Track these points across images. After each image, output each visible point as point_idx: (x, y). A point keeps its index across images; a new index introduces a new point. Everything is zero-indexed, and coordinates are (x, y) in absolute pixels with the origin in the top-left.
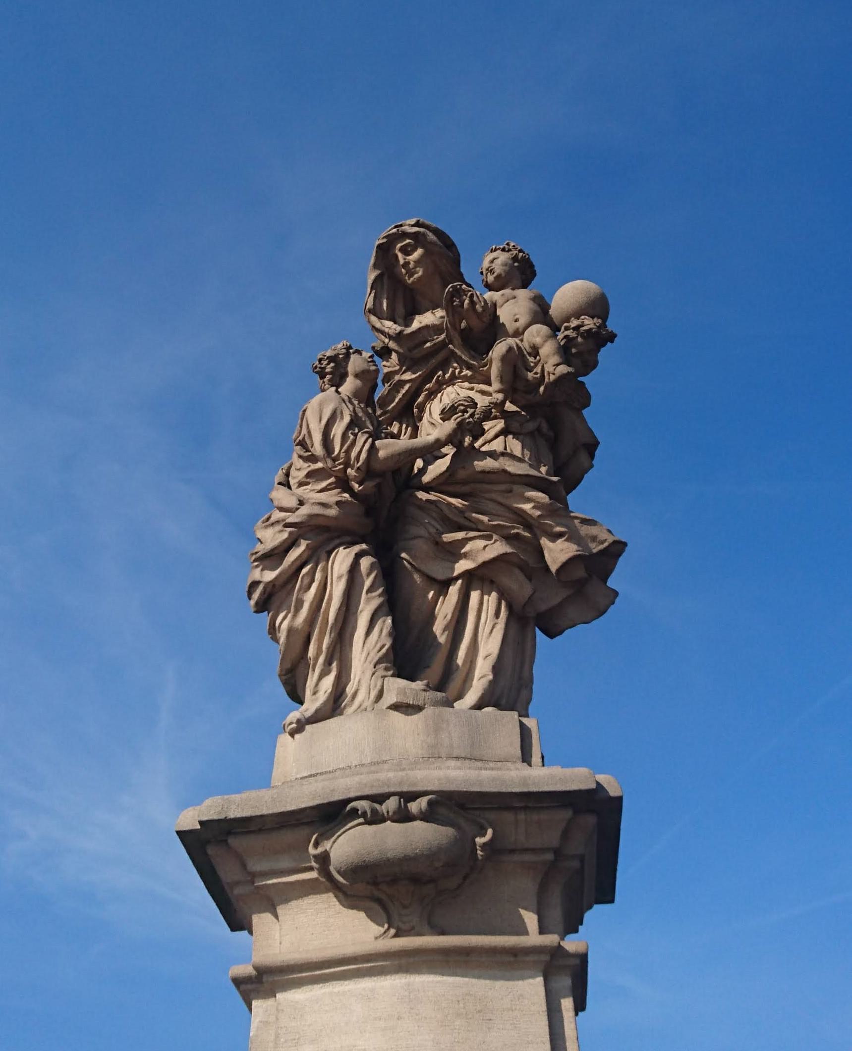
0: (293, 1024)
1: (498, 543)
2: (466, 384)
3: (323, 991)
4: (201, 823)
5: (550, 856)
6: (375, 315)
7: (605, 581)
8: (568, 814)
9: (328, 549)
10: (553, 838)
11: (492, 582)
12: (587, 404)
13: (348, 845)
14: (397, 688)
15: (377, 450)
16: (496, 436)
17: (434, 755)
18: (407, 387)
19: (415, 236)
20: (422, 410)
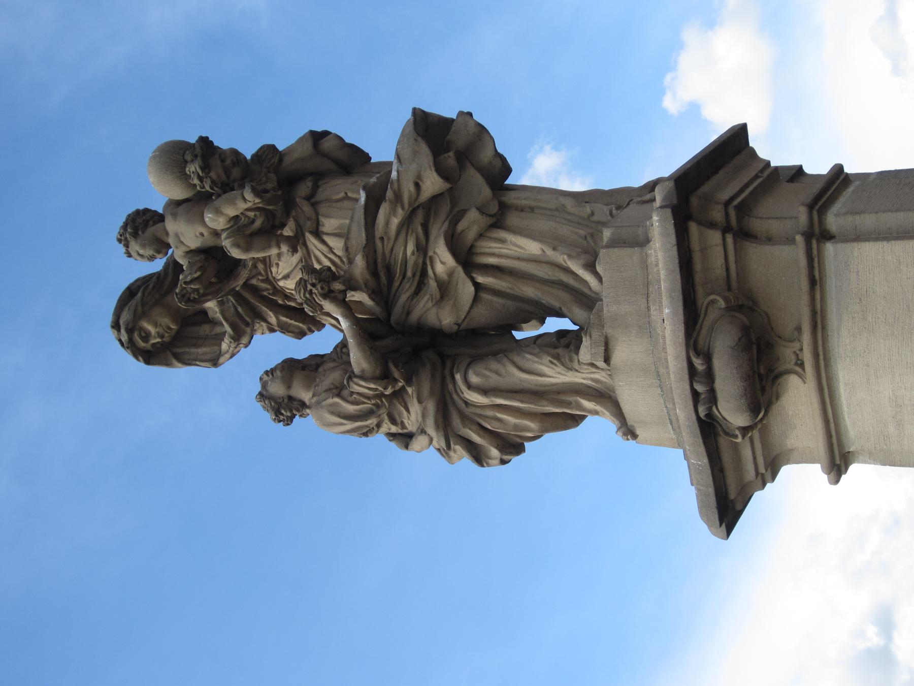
1: (438, 251)
2: (274, 269)
3: (847, 419)
4: (721, 525)
5: (730, 239)
6: (218, 359)
7: (452, 120)
8: (693, 227)
10: (715, 237)
11: (472, 246)
12: (272, 148)
15: (363, 371)
16: (324, 242)
17: (647, 329)
18: (284, 319)
19: (130, 331)
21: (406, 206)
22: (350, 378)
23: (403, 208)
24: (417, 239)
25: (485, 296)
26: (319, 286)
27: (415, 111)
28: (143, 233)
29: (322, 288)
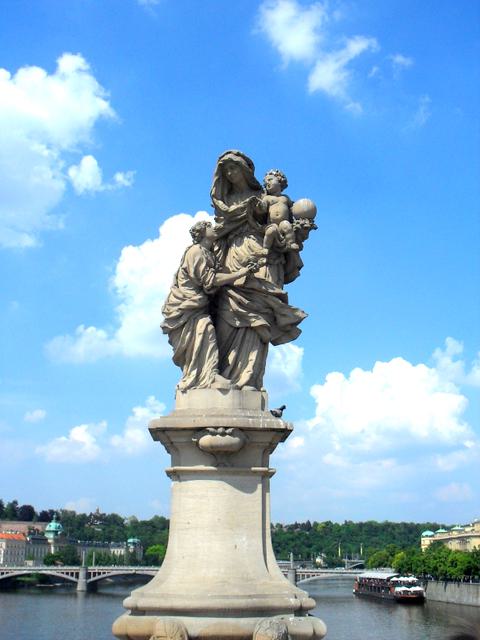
13: (206, 440)
14: (222, 381)
25: (231, 330)
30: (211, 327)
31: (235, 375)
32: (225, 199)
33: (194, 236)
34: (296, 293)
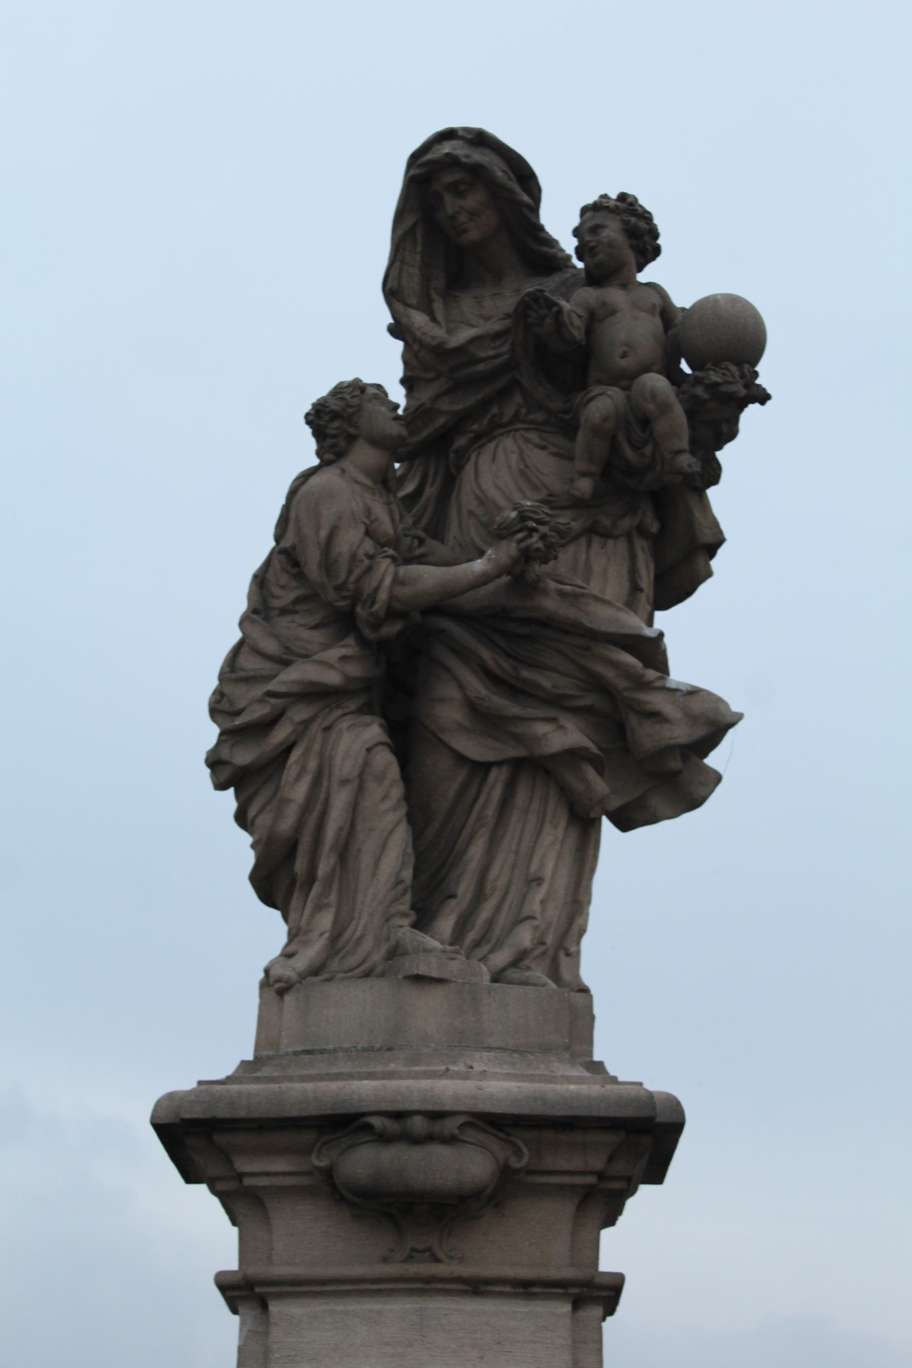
0: (290, 1340)
2: (533, 436)
5: (590, 1180)
9: (325, 725)
18: (441, 421)
20: (463, 456)
21: (627, 694)
22: (394, 559)
23: (626, 689)
24: (572, 697)
26: (540, 545)
27: (739, 717)
28: (632, 247)
29: (538, 550)
30: (385, 759)
31: (472, 936)
32: (438, 306)
33: (319, 434)
34: (697, 641)
